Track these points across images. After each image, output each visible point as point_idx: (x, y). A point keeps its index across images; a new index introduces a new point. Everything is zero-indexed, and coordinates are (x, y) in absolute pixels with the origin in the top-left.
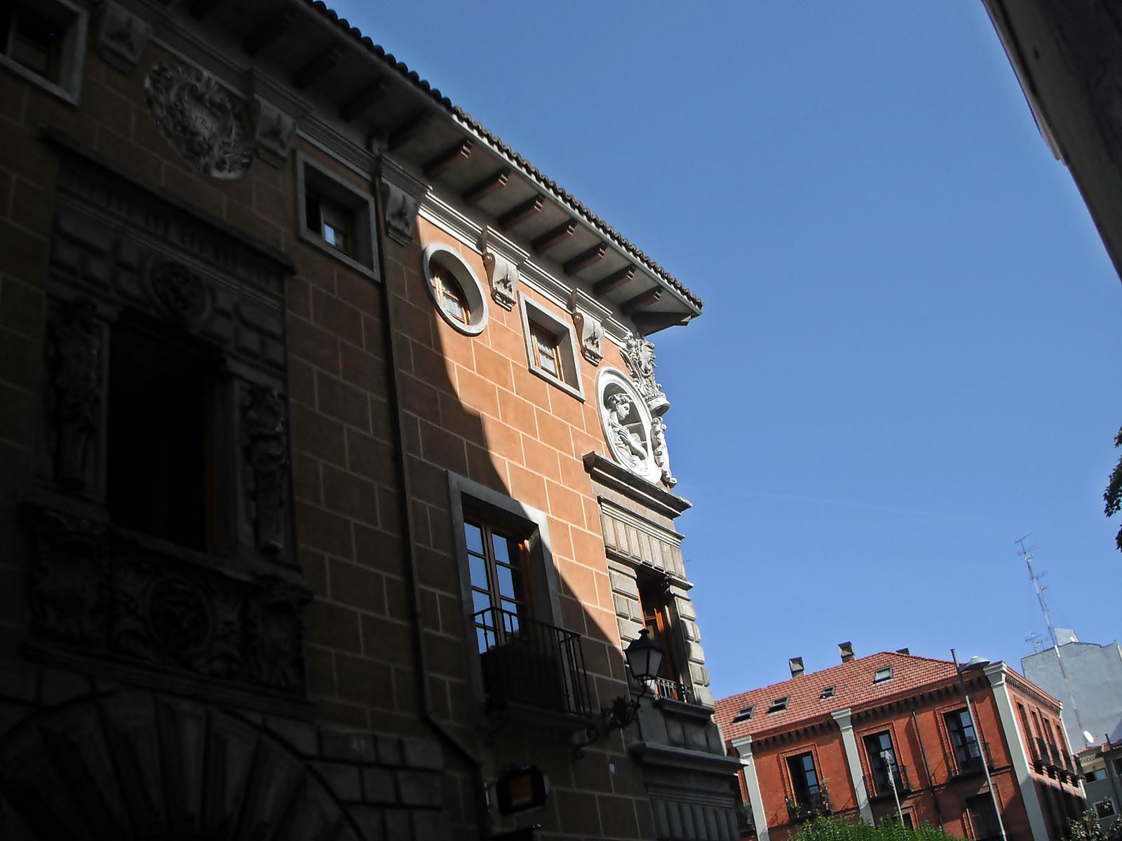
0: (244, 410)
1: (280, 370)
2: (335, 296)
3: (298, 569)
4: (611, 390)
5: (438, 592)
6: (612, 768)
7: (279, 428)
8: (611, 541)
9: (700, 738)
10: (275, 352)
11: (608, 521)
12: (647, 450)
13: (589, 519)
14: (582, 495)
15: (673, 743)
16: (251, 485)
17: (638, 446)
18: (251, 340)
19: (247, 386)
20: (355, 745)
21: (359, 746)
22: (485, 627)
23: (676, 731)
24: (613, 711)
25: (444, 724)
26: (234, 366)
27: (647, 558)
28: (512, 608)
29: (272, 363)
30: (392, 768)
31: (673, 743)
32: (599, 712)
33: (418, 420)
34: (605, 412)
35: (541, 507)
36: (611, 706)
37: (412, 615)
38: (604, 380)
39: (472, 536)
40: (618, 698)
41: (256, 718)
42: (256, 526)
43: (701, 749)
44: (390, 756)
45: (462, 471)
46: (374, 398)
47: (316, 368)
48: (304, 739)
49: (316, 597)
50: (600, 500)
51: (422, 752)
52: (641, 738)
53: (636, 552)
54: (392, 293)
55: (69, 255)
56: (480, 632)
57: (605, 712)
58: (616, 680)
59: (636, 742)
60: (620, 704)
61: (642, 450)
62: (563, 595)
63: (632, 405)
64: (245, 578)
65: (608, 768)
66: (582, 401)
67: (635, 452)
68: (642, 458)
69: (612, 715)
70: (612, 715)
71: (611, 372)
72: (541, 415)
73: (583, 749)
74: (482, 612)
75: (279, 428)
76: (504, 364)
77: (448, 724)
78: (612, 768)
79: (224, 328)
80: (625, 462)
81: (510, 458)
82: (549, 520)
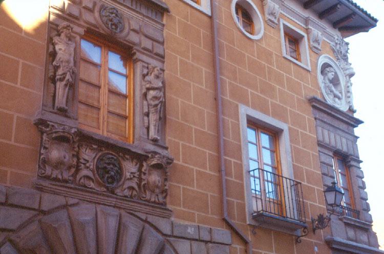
1: (161, 57)
2: (189, 23)
4: (326, 66)
5: (233, 160)
6: (316, 249)
7: (160, 84)
8: (321, 138)
9: (364, 237)
10: (159, 49)
11: (320, 129)
12: (342, 95)
13: (310, 127)
14: (307, 117)
15: (349, 239)
17: (337, 93)
18: (147, 44)
19: (146, 65)
20: (189, 230)
21: (191, 231)
22: (254, 177)
23: (351, 233)
24: (317, 220)
25: (232, 222)
26: (138, 55)
27: (339, 147)
28: (270, 169)
29: (157, 54)
30: (206, 242)
31: (349, 239)
32: (310, 220)
33: (227, 82)
34: (320, 77)
35: (286, 121)
36: (316, 218)
37: (220, 171)
38: (322, 60)
39: (251, 134)
40: (320, 214)
43: (365, 244)
44: (205, 236)
45: (247, 104)
46: (205, 71)
47: (179, 57)
48: (166, 228)
49: (174, 161)
50: (316, 119)
51: (222, 234)
52: (332, 236)
53: (333, 143)
54: (216, 21)
56: (252, 179)
57: (313, 221)
58: (319, 205)
59: (329, 237)
60: (321, 219)
61: (340, 95)
62: (294, 163)
63: (336, 73)
64: (140, 152)
65: (314, 248)
66: (308, 71)
67: (335, 96)
68: (339, 98)
69: (317, 222)
70: (317, 222)
71: (325, 57)
72: (288, 78)
73: (302, 238)
74: (254, 170)
75: (160, 84)
76: (271, 54)
77: (235, 222)
78: (316, 249)
79: (134, 38)
80: (330, 100)
81: (271, 98)
82: (290, 129)
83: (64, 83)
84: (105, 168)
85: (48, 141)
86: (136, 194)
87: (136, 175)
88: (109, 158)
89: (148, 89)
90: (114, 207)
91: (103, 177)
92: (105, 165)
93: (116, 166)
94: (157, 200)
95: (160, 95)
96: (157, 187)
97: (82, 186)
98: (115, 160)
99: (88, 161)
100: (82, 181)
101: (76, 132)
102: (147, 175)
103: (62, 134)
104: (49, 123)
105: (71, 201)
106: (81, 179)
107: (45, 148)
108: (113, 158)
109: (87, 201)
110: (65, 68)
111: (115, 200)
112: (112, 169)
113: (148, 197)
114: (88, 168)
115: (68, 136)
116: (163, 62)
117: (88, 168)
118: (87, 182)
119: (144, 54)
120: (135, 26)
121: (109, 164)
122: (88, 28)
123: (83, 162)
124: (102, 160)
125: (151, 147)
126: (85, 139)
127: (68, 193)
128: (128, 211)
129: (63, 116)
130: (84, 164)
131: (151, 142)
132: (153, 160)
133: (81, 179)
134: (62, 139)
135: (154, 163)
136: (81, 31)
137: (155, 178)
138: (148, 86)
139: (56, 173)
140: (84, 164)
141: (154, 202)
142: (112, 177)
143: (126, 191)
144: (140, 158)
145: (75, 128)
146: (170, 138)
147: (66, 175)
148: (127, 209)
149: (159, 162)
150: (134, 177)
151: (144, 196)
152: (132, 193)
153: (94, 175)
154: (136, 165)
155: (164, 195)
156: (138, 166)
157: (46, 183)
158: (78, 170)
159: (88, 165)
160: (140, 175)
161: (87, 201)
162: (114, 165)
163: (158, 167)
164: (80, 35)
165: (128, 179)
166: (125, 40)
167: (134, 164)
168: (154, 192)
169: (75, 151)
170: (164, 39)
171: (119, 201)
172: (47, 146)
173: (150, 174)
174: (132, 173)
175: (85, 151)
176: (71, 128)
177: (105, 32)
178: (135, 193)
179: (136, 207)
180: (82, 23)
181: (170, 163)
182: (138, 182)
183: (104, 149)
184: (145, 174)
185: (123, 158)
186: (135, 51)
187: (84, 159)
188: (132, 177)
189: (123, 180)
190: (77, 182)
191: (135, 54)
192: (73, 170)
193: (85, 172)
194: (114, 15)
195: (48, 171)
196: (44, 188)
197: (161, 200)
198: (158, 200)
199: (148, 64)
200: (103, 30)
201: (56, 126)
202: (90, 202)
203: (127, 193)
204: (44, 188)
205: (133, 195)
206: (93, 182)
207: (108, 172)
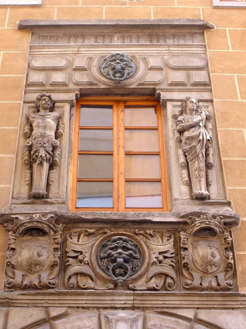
0: (175, 117)
1: (205, 86)
3: (229, 204)
10: (200, 77)
16: (182, 160)
18: (179, 76)
26: (164, 96)
29: (196, 84)
41: (189, 314)
42: (190, 184)
49: (243, 219)
55: (36, 77)
83: (38, 162)
84: (109, 256)
85: (15, 239)
86: (171, 281)
87: (167, 255)
88: (114, 241)
89: (181, 132)
90: (133, 308)
91: (108, 269)
92: (109, 251)
93: (128, 249)
94: (214, 284)
95: (198, 133)
96: (211, 264)
97: (72, 288)
98: (125, 241)
99: (81, 253)
100: (73, 280)
101: (52, 217)
102: (190, 250)
103: (29, 225)
104: (13, 216)
105: (54, 313)
106: (70, 277)
107: (13, 249)
108: (121, 239)
109: (83, 308)
110: (38, 144)
111: (132, 298)
112: (120, 254)
113: (196, 283)
114: (81, 261)
115: (40, 225)
116: (211, 91)
117: (81, 261)
118: (83, 281)
119: (172, 91)
120: (153, 62)
121: (116, 248)
122: (80, 89)
123: (75, 255)
124: (104, 246)
125: (196, 208)
126: (71, 223)
127: (49, 302)
128: (159, 310)
129: (42, 204)
130: (75, 257)
131: (197, 202)
132: (194, 226)
133: (70, 277)
134: (35, 231)
135: (196, 229)
136: (72, 96)
137: (203, 252)
138: (178, 127)
139: (33, 279)
140: (75, 257)
141: (210, 288)
142: (120, 266)
143: (153, 280)
144: (173, 229)
145: (50, 213)
146: (231, 188)
147: (45, 277)
148: (157, 308)
149: (203, 225)
150: (165, 257)
151: (189, 282)
152: (165, 282)
153: (94, 270)
154: (168, 240)
155: (231, 273)
156: (172, 240)
157: (15, 294)
158: (64, 267)
159: (80, 257)
160: (177, 254)
161: (83, 308)
162: (125, 248)
163: (207, 232)
164: (71, 102)
165: (154, 263)
166: (140, 84)
167: (165, 239)
168: (207, 273)
169: (58, 244)
170: (207, 64)
171: (138, 298)
172: (13, 246)
173: (194, 247)
174: (160, 253)
175: (78, 241)
176: (44, 215)
177: (107, 85)
178: (169, 280)
179: (173, 301)
180: (72, 86)
181: (236, 223)
182: (173, 264)
183: (108, 231)
184: (186, 249)
185: (147, 236)
186: (157, 92)
187: (75, 251)
188: (161, 257)
189: (145, 265)
190: (66, 284)
191: (159, 94)
192: (56, 269)
193: (76, 268)
194: (118, 61)
195: (18, 278)
196: (10, 301)
197: (223, 283)
198: (218, 284)
199: (181, 101)
200: (104, 84)
201: (21, 217)
202: (88, 308)
203: (153, 283)
204: (10, 301)
205: (167, 285)
206: (92, 279)
207: (114, 261)
